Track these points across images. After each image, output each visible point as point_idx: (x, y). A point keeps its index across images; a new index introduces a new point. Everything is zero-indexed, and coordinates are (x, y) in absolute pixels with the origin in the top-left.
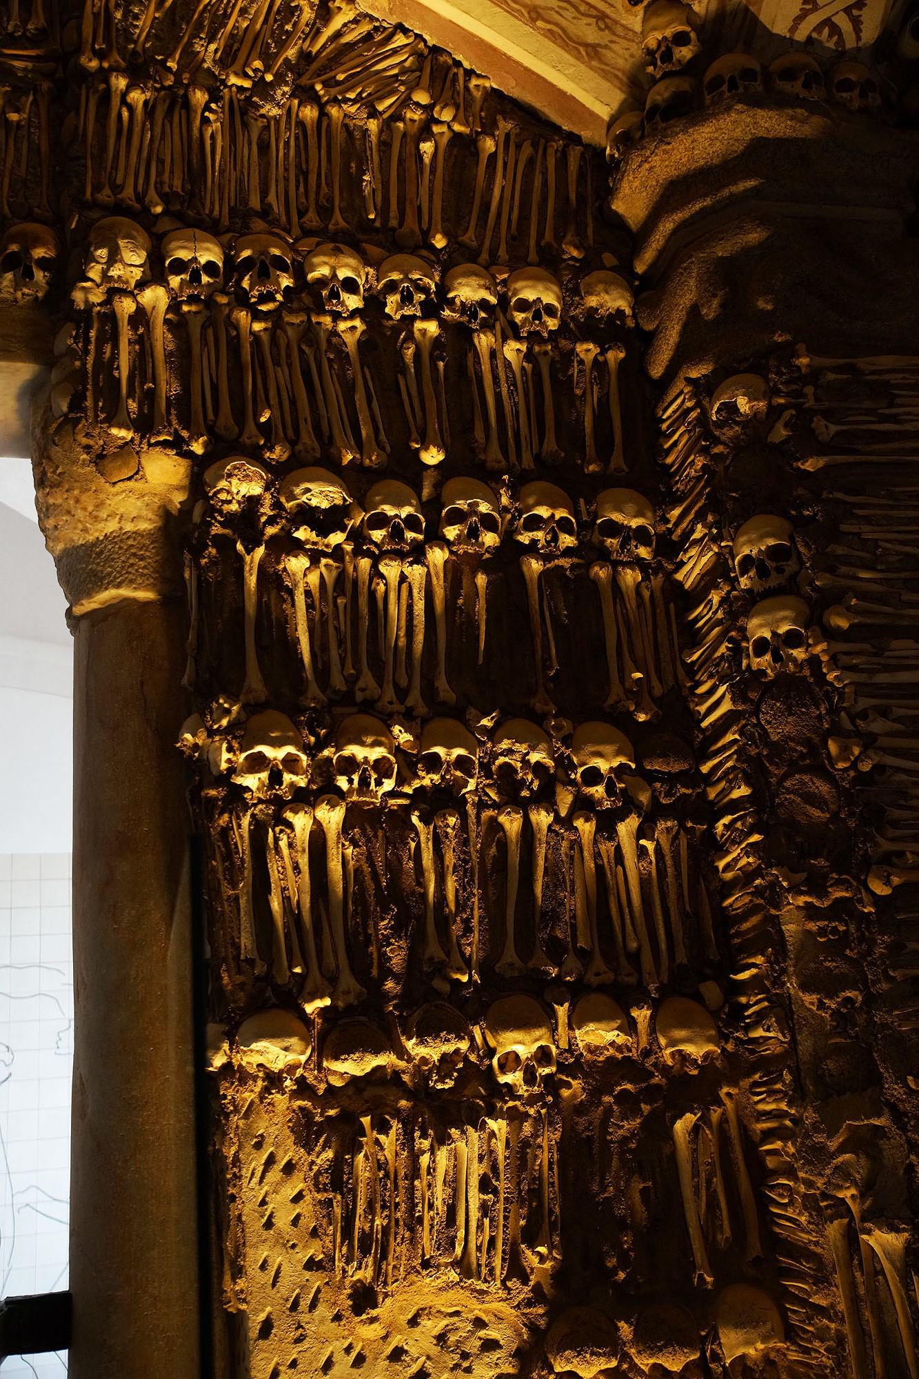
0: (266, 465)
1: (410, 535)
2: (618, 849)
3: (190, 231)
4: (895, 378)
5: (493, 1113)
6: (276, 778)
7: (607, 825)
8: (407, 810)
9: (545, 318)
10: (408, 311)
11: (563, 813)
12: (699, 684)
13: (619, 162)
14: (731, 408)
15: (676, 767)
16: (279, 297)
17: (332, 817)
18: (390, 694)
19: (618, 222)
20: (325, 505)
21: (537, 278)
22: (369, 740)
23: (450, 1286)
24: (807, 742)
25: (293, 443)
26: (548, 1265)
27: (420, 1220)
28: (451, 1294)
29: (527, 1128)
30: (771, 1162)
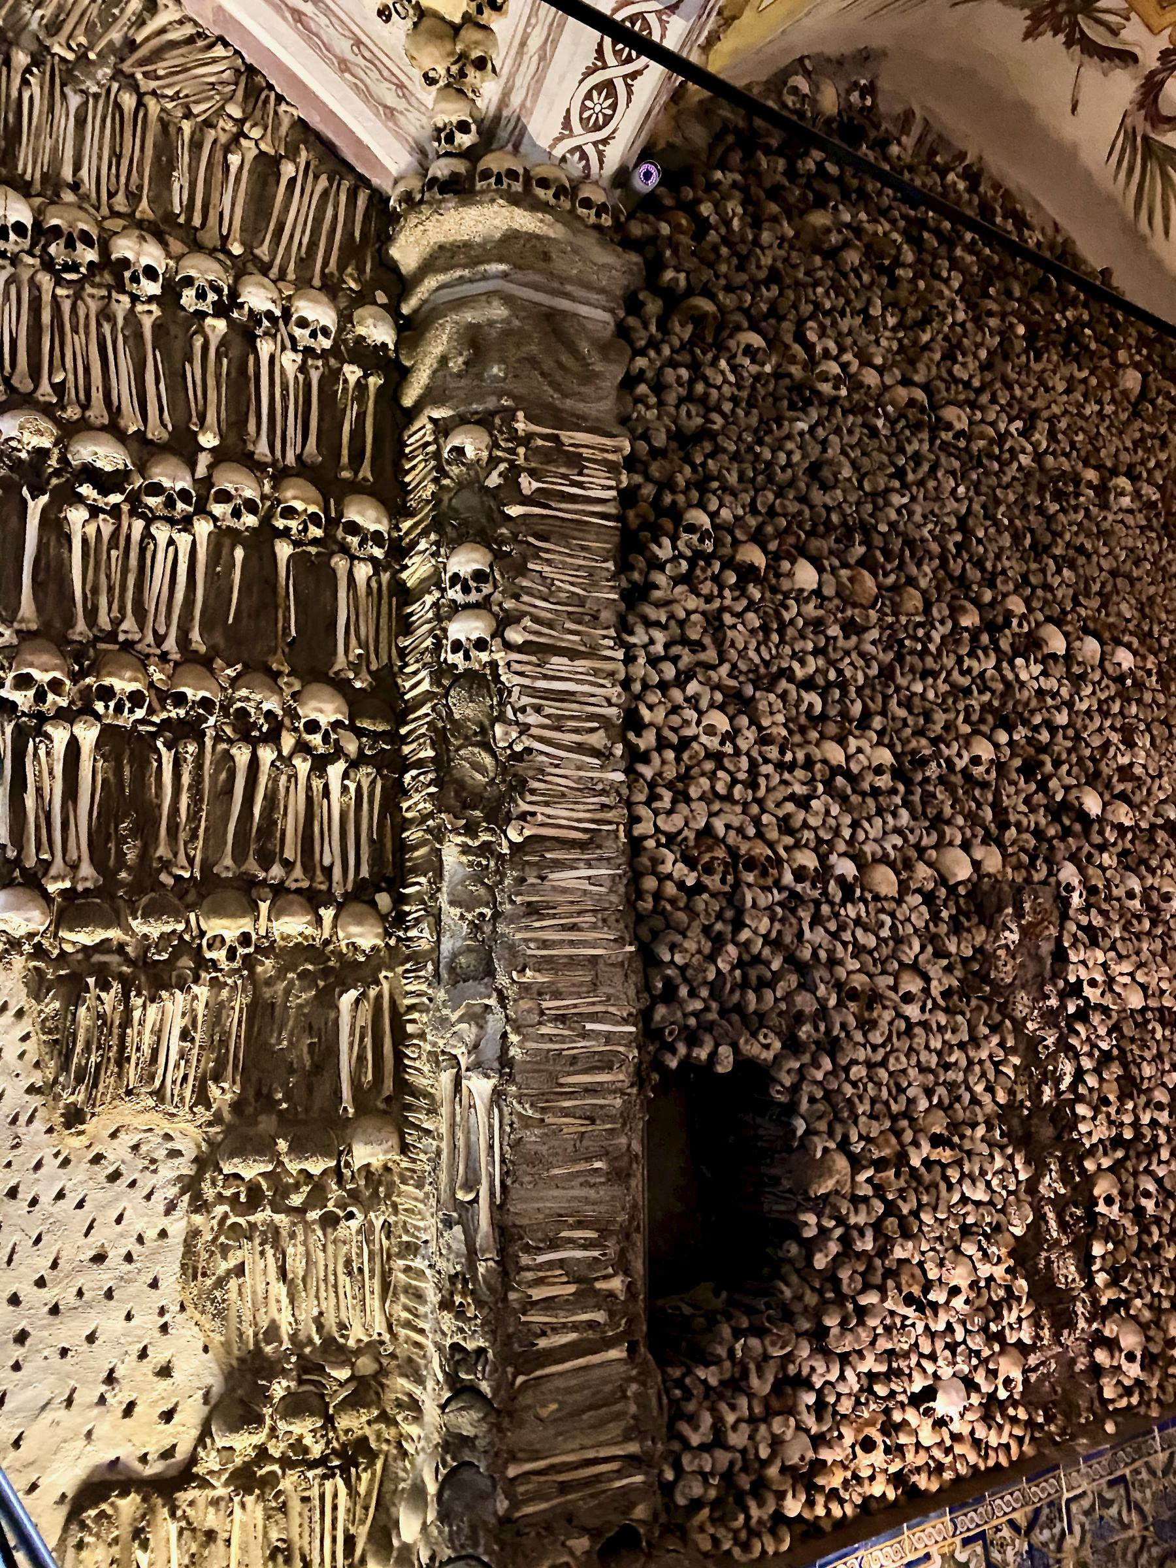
0: (57, 422)
1: (180, 505)
2: (326, 786)
5: (196, 980)
6: (40, 697)
7: (320, 764)
8: (154, 736)
10: (203, 306)
11: (285, 753)
12: (406, 665)
13: (399, 216)
16: (83, 270)
17: (88, 734)
18: (150, 639)
19: (392, 267)
20: (109, 468)
21: (316, 301)
22: (128, 674)
23: (146, 1110)
24: (481, 725)
26: (228, 1096)
27: (128, 1059)
28: (147, 1116)
29: (225, 993)
30: (410, 1028)
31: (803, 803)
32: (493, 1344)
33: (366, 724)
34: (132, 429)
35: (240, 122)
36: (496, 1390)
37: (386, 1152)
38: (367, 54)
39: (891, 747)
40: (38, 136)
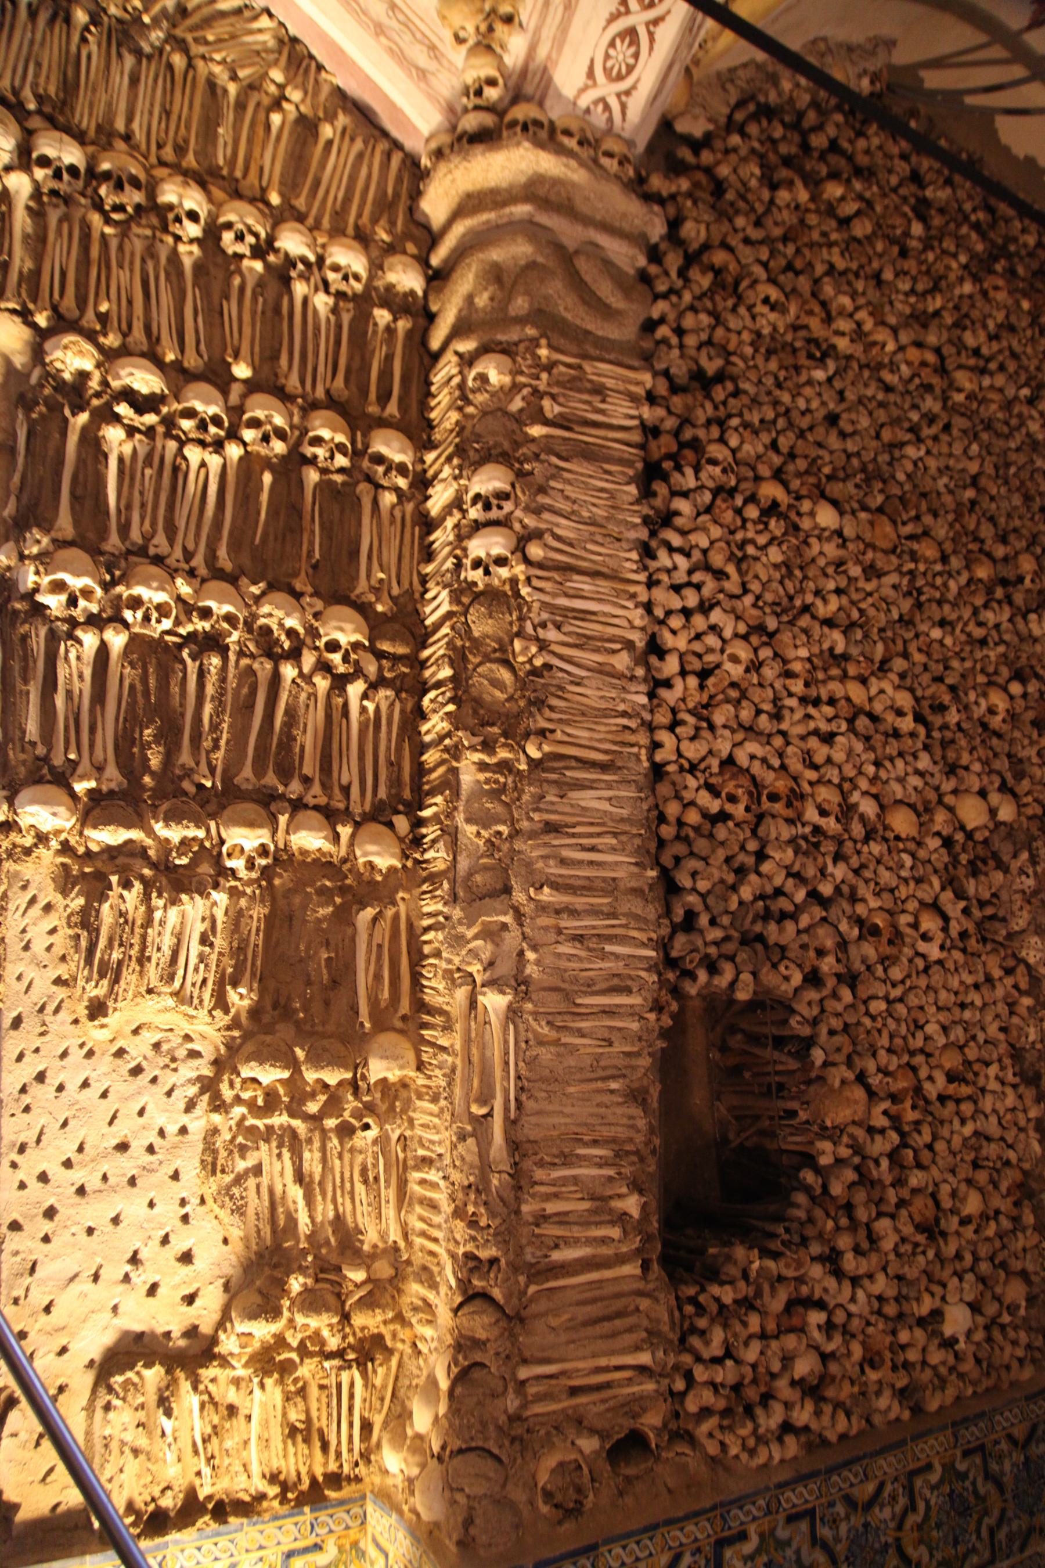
0: (100, 348)
1: (213, 430)
2: (346, 705)
3: (57, 134)
4: (610, 383)
5: (216, 886)
6: (72, 602)
7: (340, 682)
8: (180, 647)
9: (352, 281)
11: (306, 669)
12: (426, 591)
14: (483, 378)
15: (401, 650)
17: (117, 640)
18: (178, 553)
20: (145, 390)
21: (350, 248)
22: (155, 584)
23: (166, 1010)
24: (499, 641)
25: (125, 335)
26: (246, 1003)
27: (149, 959)
28: (168, 1015)
29: (243, 902)
30: (427, 949)
31: (828, 738)
32: (506, 1254)
33: (385, 646)
34: (170, 357)
35: (281, 87)
36: (508, 1296)
37: (401, 1068)
38: (401, 17)
39: (912, 690)
40: (94, 90)
